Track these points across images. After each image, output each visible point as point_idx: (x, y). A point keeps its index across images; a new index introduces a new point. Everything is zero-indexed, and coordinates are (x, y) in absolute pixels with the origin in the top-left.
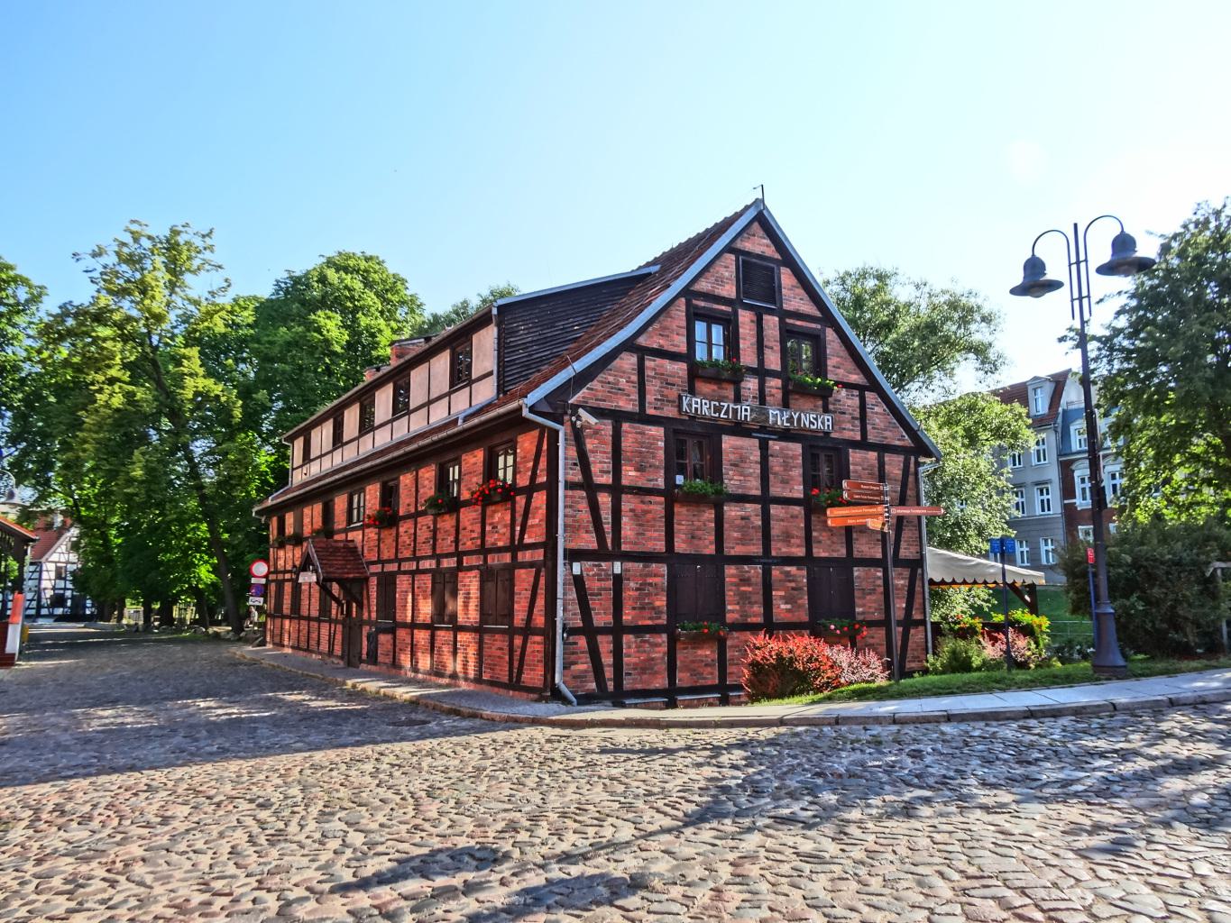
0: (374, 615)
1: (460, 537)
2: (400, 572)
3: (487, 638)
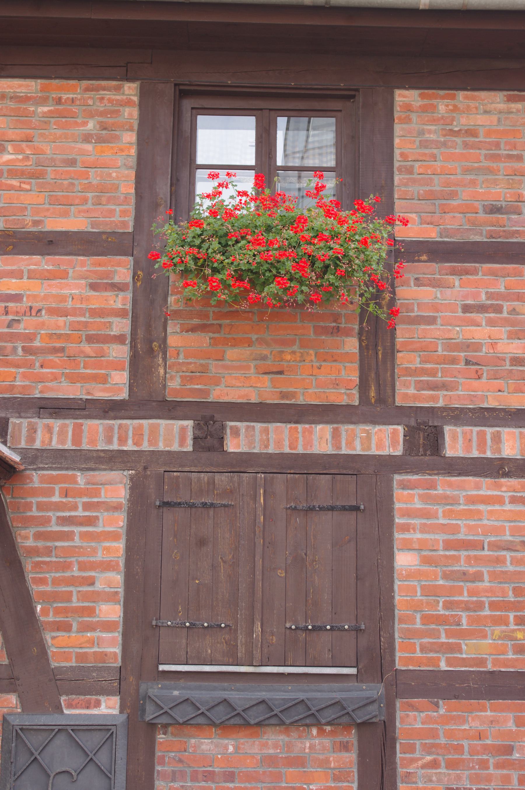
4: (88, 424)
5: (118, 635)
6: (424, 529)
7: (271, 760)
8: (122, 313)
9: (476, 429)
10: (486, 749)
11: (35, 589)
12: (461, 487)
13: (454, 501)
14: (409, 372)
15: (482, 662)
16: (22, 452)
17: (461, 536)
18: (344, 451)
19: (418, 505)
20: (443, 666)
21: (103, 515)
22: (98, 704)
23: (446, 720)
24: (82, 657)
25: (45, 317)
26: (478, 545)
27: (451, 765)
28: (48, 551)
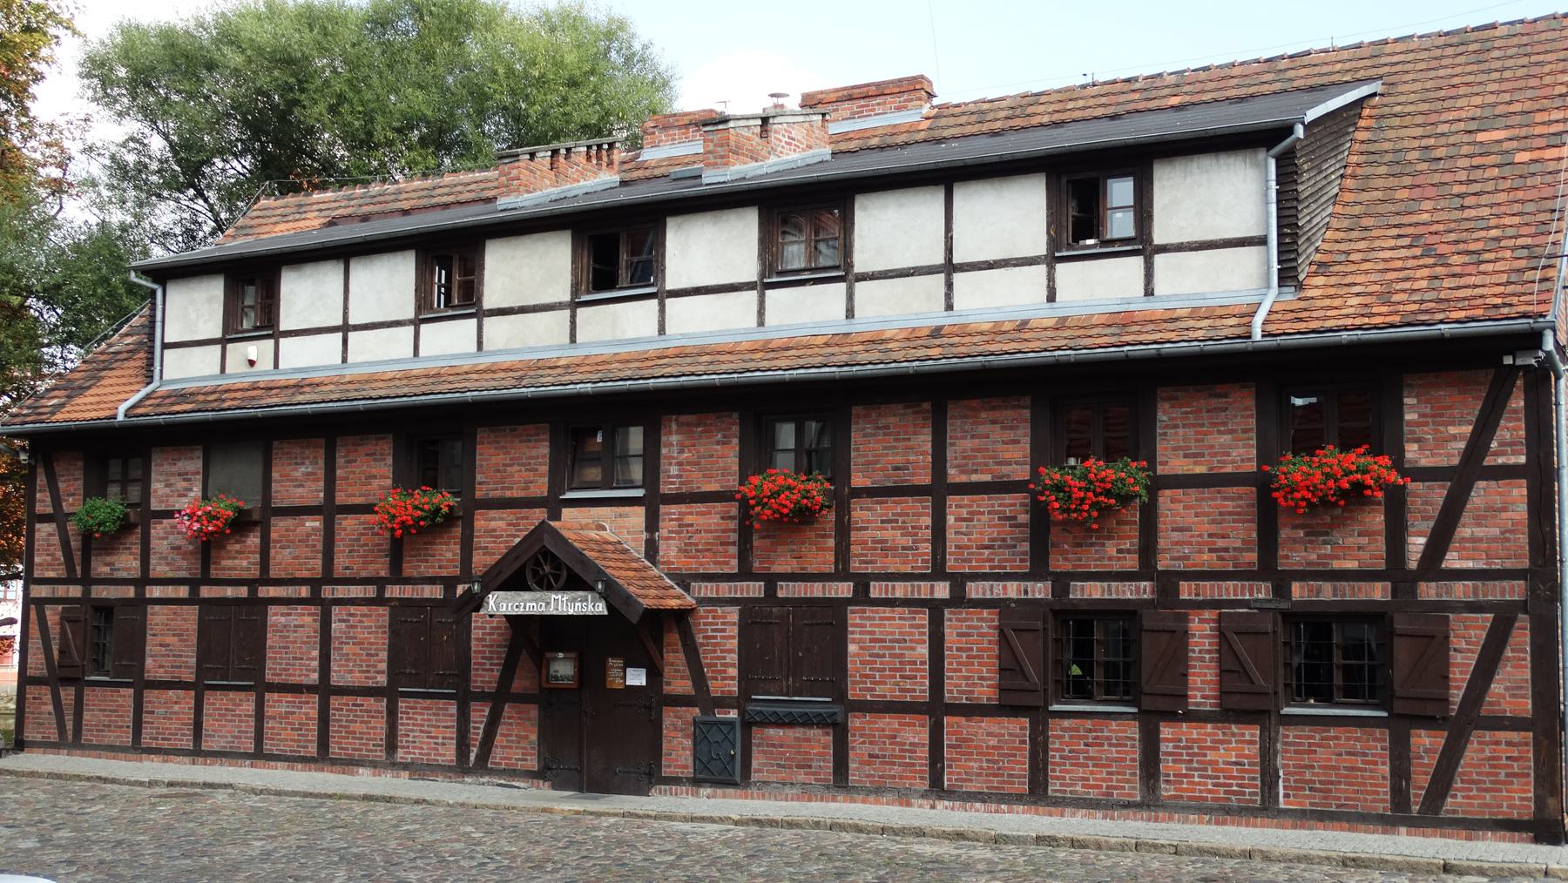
0: (726, 681)
1: (1162, 543)
2: (862, 596)
3: (1289, 734)
4: (722, 585)
5: (736, 682)
6: (861, 633)
7: (797, 739)
8: (734, 531)
10: (885, 736)
11: (704, 661)
12: (877, 612)
13: (874, 619)
15: (885, 696)
16: (696, 599)
19: (858, 621)
23: (869, 723)
24: (722, 692)
25: (703, 534)
26: (884, 641)
27: (870, 743)
28: (708, 645)
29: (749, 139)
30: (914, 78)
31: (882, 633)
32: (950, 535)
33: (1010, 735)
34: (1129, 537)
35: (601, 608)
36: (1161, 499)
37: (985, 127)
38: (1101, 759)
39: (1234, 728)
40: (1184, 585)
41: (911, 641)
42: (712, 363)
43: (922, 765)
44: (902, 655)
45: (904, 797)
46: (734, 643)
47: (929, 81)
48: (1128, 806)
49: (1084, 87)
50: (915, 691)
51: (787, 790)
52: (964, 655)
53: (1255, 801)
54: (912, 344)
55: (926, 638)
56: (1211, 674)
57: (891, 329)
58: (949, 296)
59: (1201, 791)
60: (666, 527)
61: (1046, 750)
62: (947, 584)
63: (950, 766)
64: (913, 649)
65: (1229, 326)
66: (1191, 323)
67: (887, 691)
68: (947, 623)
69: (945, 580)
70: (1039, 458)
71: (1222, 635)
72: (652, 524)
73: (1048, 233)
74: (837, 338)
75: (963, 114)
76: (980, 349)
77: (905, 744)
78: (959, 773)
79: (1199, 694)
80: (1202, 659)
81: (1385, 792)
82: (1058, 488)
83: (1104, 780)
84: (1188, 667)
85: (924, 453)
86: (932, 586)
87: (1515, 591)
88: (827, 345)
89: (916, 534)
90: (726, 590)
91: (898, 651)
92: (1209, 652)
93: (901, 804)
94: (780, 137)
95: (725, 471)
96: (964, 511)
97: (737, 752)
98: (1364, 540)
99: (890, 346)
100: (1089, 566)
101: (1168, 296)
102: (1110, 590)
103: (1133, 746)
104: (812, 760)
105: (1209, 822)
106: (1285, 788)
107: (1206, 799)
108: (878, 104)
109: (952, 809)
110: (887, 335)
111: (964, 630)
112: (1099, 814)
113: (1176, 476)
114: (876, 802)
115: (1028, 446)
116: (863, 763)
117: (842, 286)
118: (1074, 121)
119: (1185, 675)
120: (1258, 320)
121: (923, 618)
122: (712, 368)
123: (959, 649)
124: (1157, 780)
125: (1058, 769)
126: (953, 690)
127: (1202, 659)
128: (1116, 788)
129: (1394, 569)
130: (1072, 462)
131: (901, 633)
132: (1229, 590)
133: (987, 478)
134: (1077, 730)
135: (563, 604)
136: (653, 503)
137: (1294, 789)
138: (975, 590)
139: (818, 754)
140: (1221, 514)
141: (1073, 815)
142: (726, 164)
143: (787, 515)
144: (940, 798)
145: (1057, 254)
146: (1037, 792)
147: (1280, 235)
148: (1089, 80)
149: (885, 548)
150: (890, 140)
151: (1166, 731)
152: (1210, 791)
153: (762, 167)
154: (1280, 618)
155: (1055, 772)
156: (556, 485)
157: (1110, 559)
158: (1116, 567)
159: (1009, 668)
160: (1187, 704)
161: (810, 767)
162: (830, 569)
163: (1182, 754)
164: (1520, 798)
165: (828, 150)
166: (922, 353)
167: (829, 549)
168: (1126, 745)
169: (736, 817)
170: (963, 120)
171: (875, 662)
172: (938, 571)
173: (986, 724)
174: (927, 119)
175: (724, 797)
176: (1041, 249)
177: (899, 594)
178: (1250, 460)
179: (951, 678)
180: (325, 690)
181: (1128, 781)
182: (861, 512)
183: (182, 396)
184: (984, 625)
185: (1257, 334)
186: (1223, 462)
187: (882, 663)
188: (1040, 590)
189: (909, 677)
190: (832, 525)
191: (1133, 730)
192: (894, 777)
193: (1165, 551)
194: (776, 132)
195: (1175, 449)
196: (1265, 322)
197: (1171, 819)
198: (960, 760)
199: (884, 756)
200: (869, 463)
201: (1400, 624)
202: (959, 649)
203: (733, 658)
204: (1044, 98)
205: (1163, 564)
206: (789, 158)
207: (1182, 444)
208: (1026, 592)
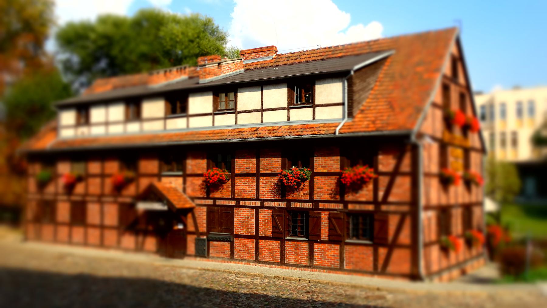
0: (203, 228)
1: (315, 192)
2: (238, 205)
3: (347, 248)
6: (238, 215)
7: (221, 245)
9: (243, 201)
10: (244, 245)
12: (242, 209)
14: (236, 193)
15: (244, 234)
17: (241, 216)
18: (229, 204)
19: (237, 212)
20: (240, 234)
21: (204, 213)
22: (203, 237)
23: (239, 241)
27: (240, 247)
29: (214, 70)
30: (271, 46)
31: (243, 215)
32: (260, 188)
33: (276, 245)
34: (307, 190)
35: (165, 208)
36: (315, 179)
37: (288, 62)
38: (298, 253)
39: (333, 246)
40: (320, 204)
41: (251, 218)
42: (198, 137)
43: (253, 253)
44: (248, 222)
45: (248, 262)
46: (205, 217)
47: (276, 47)
48: (305, 267)
49: (317, 49)
50: (251, 232)
51: (220, 260)
52: (264, 222)
53: (338, 267)
54: (250, 133)
55: (254, 217)
56: (327, 230)
57: (246, 128)
58: (262, 118)
59: (324, 263)
60: (188, 183)
61: (285, 251)
62: (260, 202)
63: (260, 254)
64: (251, 220)
65: (331, 130)
66: (323, 129)
67: (244, 232)
68: (259, 213)
69: (259, 201)
70: (284, 167)
71: (329, 219)
72: (185, 182)
73: (288, 101)
74: (232, 130)
75: (284, 57)
76: (266, 135)
77: (248, 247)
78: (262, 256)
79: (324, 235)
80: (325, 226)
81: (371, 265)
82: (286, 176)
83: (299, 259)
84: (321, 228)
85: (254, 164)
86: (256, 202)
87: (405, 208)
88: (229, 132)
89: (252, 188)
90: (203, 202)
91: (247, 221)
92: (326, 223)
93: (248, 264)
94: (225, 68)
95: (203, 168)
96: (264, 181)
97: (206, 248)
98: (367, 193)
99: (244, 133)
100: (296, 198)
101: (319, 120)
102: (301, 205)
103: (307, 250)
104: (225, 251)
105: (326, 272)
106: (346, 263)
107: (325, 265)
108: (261, 54)
109: (261, 266)
110: (245, 130)
111: (264, 215)
112: (298, 269)
113: (319, 173)
114: (241, 264)
115: (281, 163)
116: (238, 252)
117: (234, 115)
118: (312, 61)
119: (320, 230)
120: (338, 129)
121: (253, 212)
122: (198, 139)
123: (262, 221)
124: (313, 260)
125: (288, 256)
126: (261, 234)
127: (325, 226)
128: (302, 261)
129: (375, 202)
130: (294, 167)
131: (248, 216)
132: (332, 206)
133: (270, 172)
134: (292, 245)
135: (157, 206)
136: (185, 176)
137: (348, 263)
138: (267, 204)
139: (227, 249)
140: (330, 184)
141: (291, 269)
142: (205, 78)
143: (216, 182)
144: (258, 263)
145: (290, 107)
146: (282, 263)
147: (348, 102)
148: (318, 47)
149: (244, 191)
150: (263, 66)
151: (315, 246)
152: (326, 263)
153: (218, 77)
154: (345, 214)
155: (287, 256)
156: (160, 169)
157: (302, 196)
158: (303, 198)
159: (275, 227)
160: (320, 238)
161: (224, 253)
162: (230, 197)
163: (319, 253)
164: (406, 268)
165: (243, 69)
166: (251, 136)
167: (229, 191)
168: (305, 249)
169: (199, 268)
170: (283, 59)
171: (241, 224)
172: (257, 199)
173: (269, 242)
174: (274, 59)
175: (203, 260)
176: (286, 105)
177: (247, 205)
178: (338, 168)
179: (260, 229)
180: (102, 227)
181: (305, 260)
182: (238, 180)
183: (65, 142)
184: (269, 213)
185: (337, 133)
186: (331, 169)
187: (243, 224)
188: (283, 204)
189: (250, 228)
190: (230, 184)
191: (307, 245)
192: (246, 257)
193: (316, 194)
194: (223, 66)
195: (319, 165)
196: (340, 129)
197: (316, 271)
198: (263, 252)
199: (243, 251)
200: (240, 167)
201: (376, 217)
202: (262, 221)
203: (205, 221)
204: (306, 53)
205: (315, 198)
206: (228, 74)
207: (320, 163)
208: (280, 205)
